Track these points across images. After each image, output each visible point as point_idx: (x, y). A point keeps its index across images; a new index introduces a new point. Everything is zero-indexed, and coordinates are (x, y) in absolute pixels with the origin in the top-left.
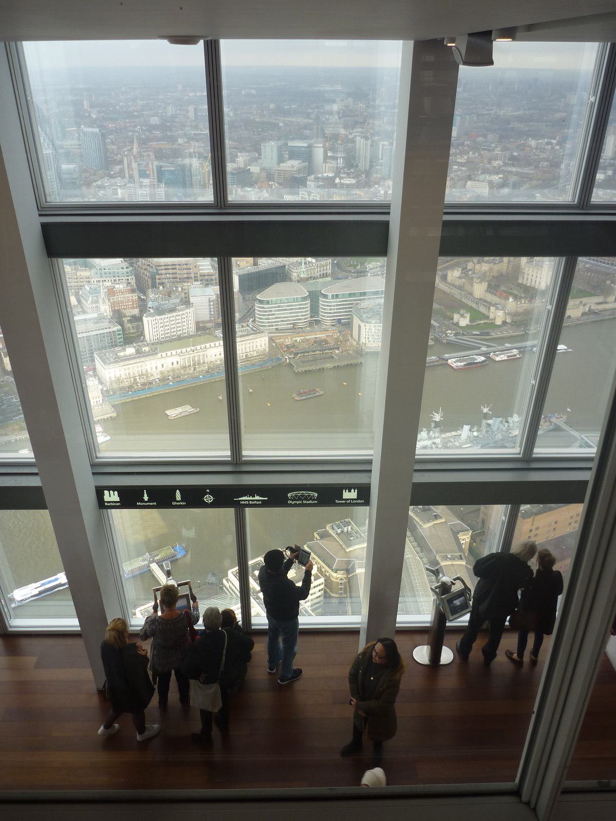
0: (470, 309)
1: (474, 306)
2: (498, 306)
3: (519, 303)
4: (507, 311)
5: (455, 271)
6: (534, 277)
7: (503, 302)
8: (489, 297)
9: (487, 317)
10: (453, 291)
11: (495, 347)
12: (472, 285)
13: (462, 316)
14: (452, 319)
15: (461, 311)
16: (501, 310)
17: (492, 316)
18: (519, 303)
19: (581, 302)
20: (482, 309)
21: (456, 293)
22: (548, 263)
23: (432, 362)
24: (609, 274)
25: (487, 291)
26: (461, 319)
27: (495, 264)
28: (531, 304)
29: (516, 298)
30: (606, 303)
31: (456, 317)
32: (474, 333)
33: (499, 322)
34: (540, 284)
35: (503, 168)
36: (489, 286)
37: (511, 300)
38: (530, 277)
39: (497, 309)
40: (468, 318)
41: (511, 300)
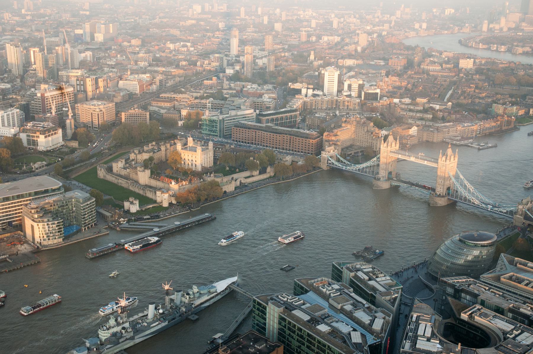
0: (137, 196)
1: (141, 192)
2: (163, 190)
7: (166, 185)
8: (154, 183)
9: (155, 202)
10: (120, 181)
11: (165, 226)
12: (137, 174)
13: (132, 203)
14: (123, 207)
17: (159, 200)
19: (232, 178)
20: (150, 195)
21: (123, 183)
23: (110, 249)
24: (251, 152)
25: (151, 177)
26: (131, 206)
27: (154, 152)
30: (253, 176)
31: (126, 205)
32: (145, 217)
33: (165, 204)
35: (149, 68)
36: (152, 173)
37: (173, 183)
39: (163, 192)
40: (138, 205)
41: (173, 183)
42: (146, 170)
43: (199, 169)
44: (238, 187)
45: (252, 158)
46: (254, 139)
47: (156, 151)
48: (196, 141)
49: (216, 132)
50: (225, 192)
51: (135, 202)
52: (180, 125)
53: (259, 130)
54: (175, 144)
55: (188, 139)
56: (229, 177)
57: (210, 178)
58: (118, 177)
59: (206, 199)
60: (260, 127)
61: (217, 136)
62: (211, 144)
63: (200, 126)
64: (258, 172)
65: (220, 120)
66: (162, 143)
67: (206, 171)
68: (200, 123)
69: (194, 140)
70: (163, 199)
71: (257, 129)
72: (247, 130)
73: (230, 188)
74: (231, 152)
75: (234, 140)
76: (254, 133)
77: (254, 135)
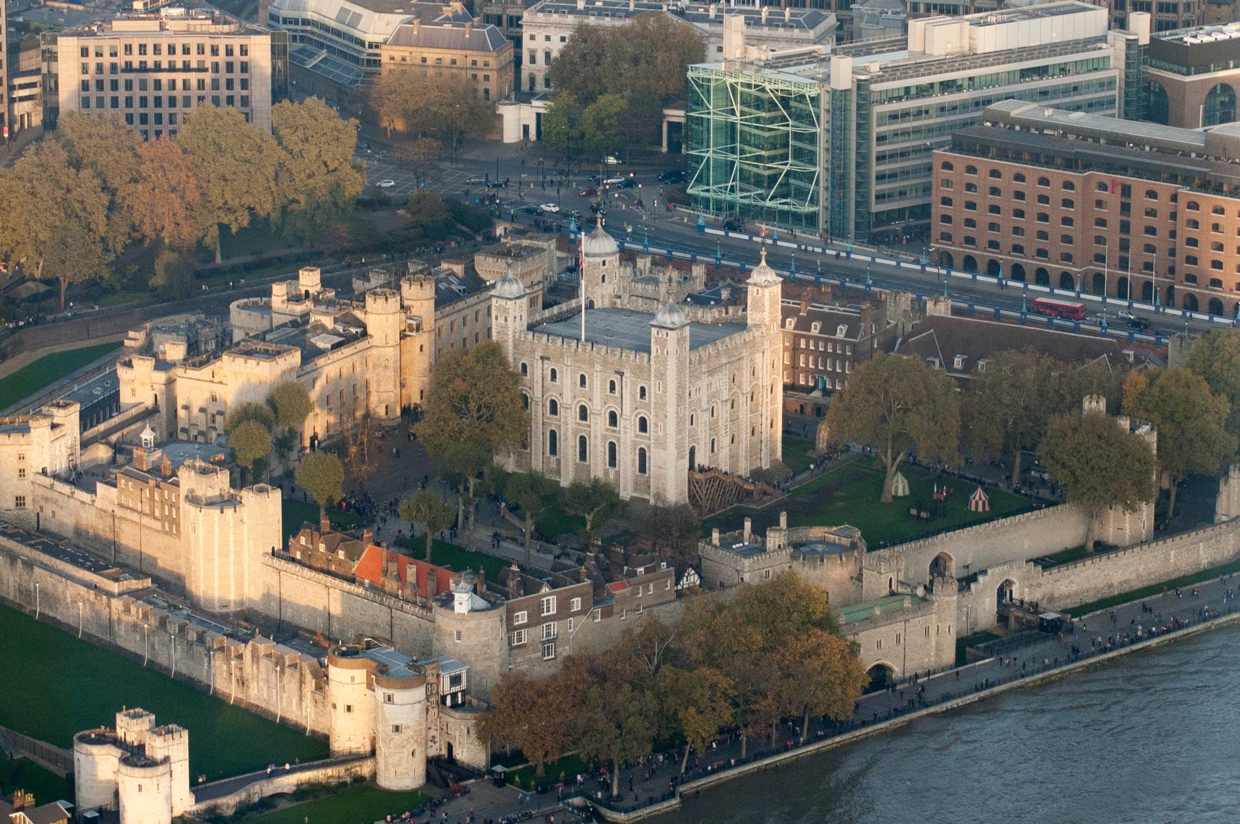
3: (522, 617)
4: (446, 687)
5: (40, 430)
6: (598, 426)
7: (410, 617)
12: (172, 525)
13: (135, 756)
15: (121, 720)
16: (406, 684)
18: (522, 617)
19: (938, 566)
22: (677, 318)
24: (1085, 351)
25: (283, 553)
28: (607, 614)
29: (495, 584)
30: (1102, 548)
33: (401, 771)
34: (643, 468)
37: (463, 601)
38: (568, 422)
40: (181, 769)
41: (463, 601)
42: (247, 496)
43: (671, 483)
44: (986, 635)
45: (1095, 405)
46: (1111, 249)
47: (322, 343)
48: (644, 263)
49: (801, 194)
50: (880, 676)
51: (157, 747)
52: (511, 134)
53: (1154, 173)
54: (475, 285)
55: (587, 245)
56: (913, 559)
57: (758, 563)
58: (25, 551)
59: (729, 733)
60: (1164, 149)
61: (811, 219)
62: (765, 289)
63: (675, 147)
64: (1147, 513)
65: (839, 97)
66: (376, 280)
67: (724, 505)
68: (676, 115)
69: (627, 257)
70: (385, 731)
71: (1141, 171)
72: (1058, 175)
73: (918, 644)
74: (926, 349)
75: (946, 260)
76: (1113, 199)
77: (1112, 214)
